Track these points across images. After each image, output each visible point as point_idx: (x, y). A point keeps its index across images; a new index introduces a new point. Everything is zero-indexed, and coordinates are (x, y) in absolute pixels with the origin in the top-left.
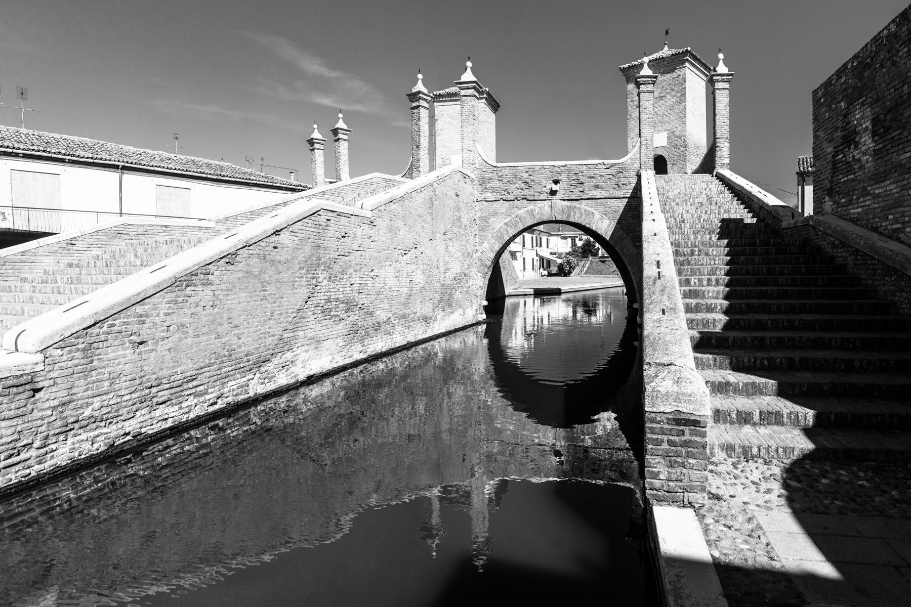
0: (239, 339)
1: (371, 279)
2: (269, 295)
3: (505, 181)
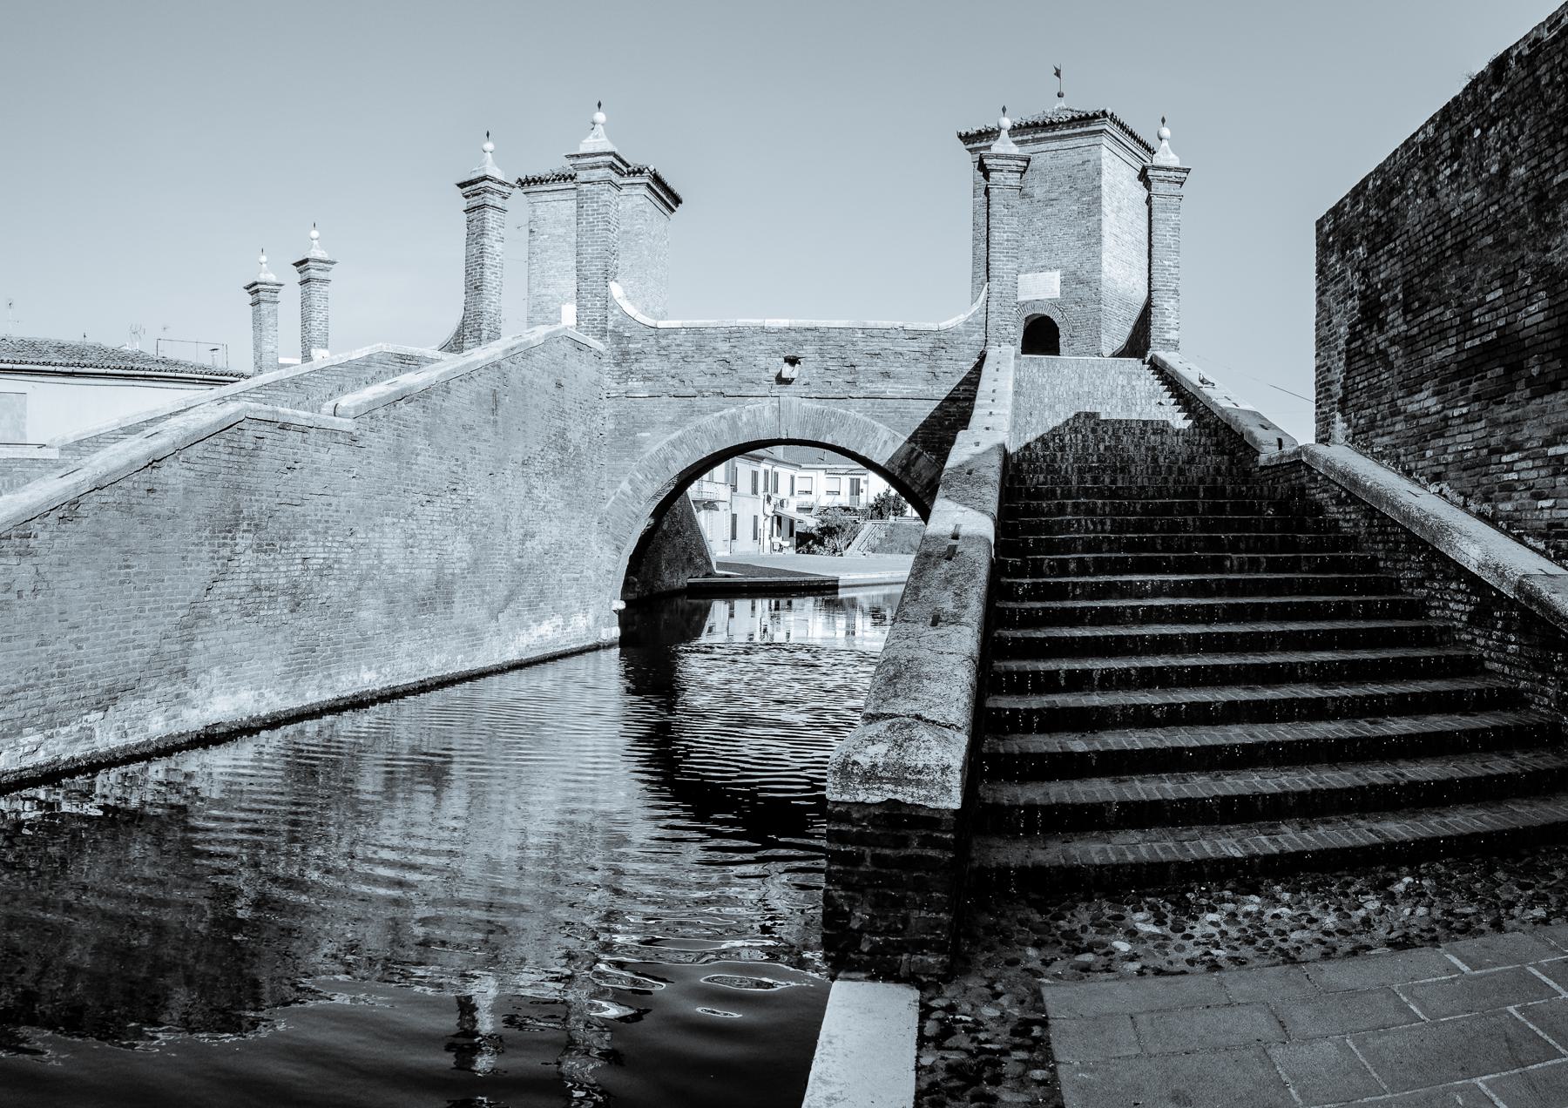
0: (80, 648)
1: (349, 550)
2: (137, 574)
3: (673, 356)
